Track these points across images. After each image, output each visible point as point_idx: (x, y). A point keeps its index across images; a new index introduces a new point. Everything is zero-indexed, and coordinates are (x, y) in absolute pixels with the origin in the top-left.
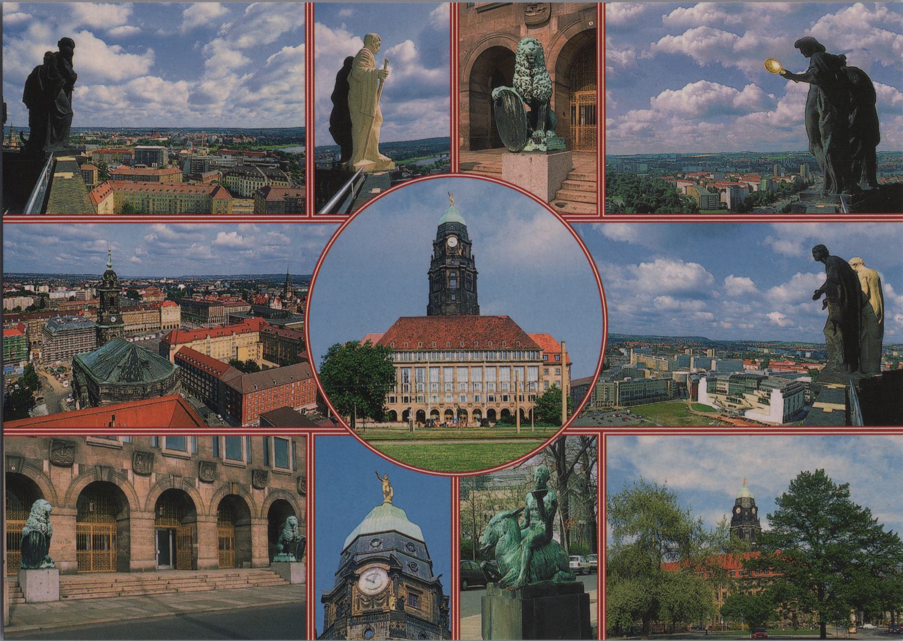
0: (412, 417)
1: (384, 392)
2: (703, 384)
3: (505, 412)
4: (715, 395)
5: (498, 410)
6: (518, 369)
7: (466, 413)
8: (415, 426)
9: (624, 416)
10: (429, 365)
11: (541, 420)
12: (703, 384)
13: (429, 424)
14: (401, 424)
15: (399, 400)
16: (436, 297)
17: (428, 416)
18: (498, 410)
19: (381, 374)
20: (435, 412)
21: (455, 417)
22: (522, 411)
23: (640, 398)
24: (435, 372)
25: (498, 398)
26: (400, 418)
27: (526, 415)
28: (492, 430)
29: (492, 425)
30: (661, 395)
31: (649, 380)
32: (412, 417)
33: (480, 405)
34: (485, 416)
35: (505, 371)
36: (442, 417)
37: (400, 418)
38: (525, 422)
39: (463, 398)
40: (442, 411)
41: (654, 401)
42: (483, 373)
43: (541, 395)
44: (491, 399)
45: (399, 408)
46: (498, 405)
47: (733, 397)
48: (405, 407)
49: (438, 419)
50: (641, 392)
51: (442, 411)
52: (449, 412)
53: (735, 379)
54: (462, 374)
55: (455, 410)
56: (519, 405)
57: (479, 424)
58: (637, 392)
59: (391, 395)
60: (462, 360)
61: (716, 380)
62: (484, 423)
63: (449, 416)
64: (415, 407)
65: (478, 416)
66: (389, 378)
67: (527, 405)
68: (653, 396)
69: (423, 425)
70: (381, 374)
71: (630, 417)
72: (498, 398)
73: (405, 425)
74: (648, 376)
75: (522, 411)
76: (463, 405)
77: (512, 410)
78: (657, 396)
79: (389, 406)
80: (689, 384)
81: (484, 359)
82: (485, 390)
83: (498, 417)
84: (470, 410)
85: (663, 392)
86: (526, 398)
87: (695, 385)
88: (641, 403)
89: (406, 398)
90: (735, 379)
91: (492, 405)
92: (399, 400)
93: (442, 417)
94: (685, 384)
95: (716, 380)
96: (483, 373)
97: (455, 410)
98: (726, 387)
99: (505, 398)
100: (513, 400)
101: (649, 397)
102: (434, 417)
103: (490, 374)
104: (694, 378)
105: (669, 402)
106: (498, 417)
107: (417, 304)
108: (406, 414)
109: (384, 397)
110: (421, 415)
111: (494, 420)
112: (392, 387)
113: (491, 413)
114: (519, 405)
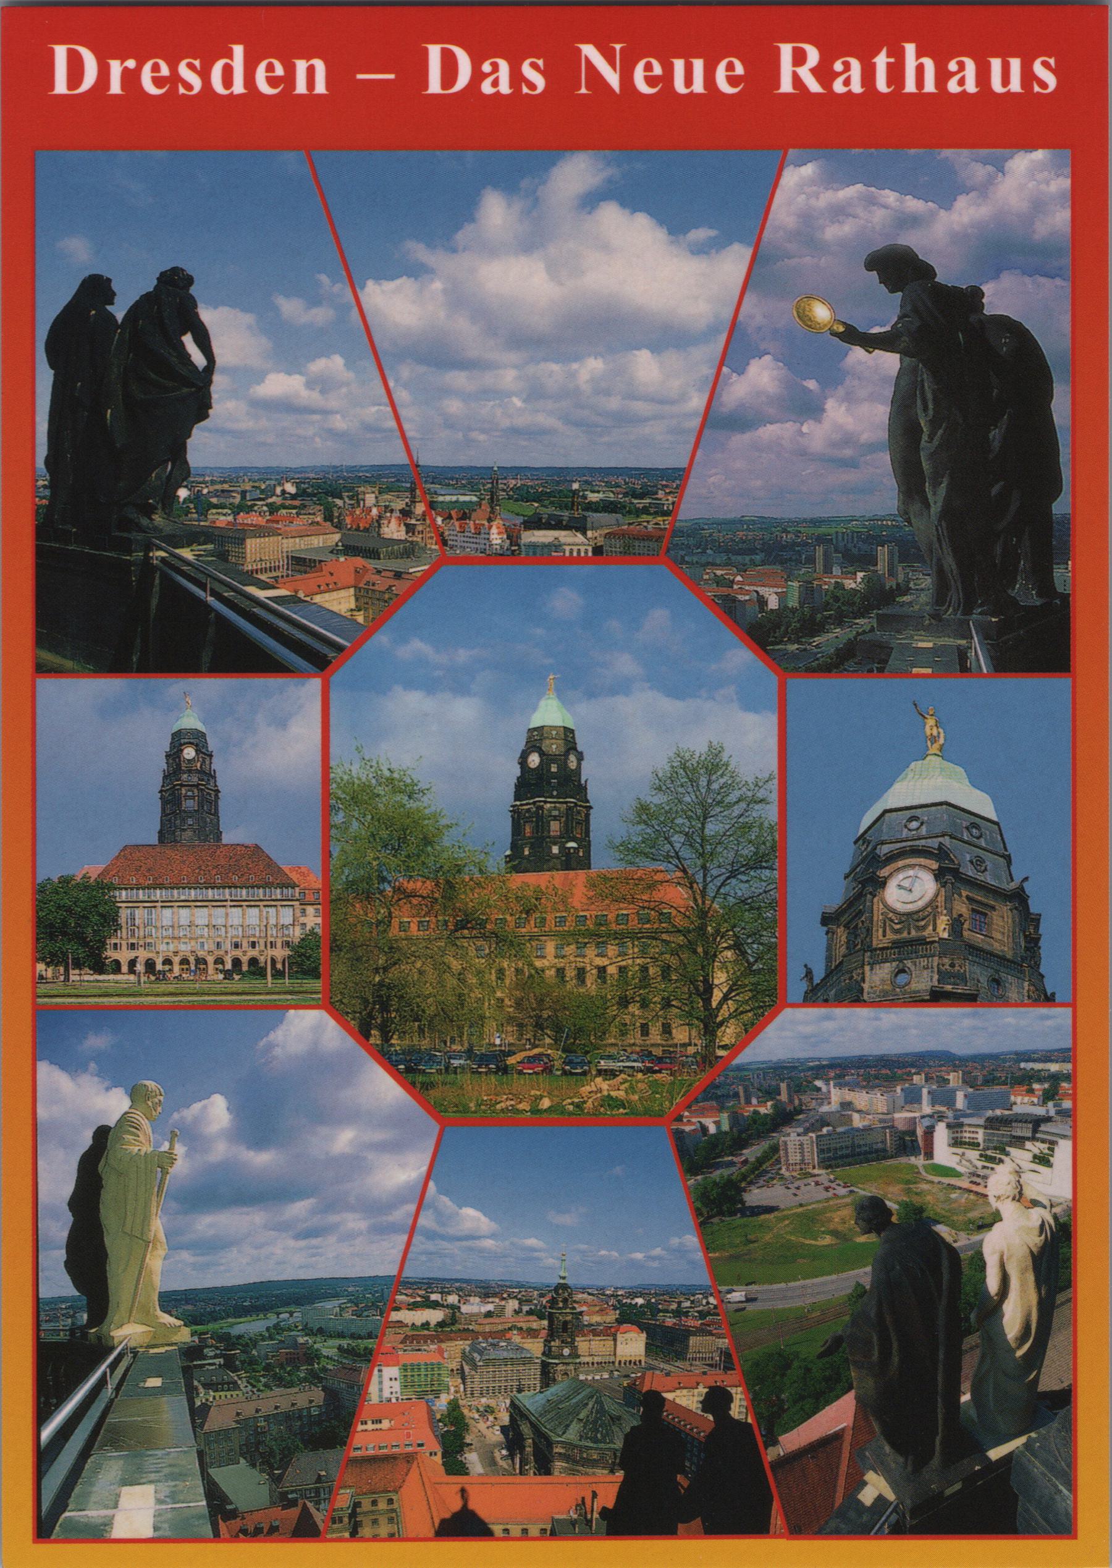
0: (140, 968)
1: (105, 937)
2: (941, 1134)
3: (253, 961)
4: (960, 1151)
5: (245, 960)
6: (270, 909)
7: (205, 963)
8: (143, 979)
9: (827, 1184)
10: (160, 904)
11: (297, 972)
12: (941, 1134)
13: (161, 977)
14: (126, 977)
15: (124, 947)
16: (170, 820)
17: (159, 967)
18: (245, 960)
19: (101, 915)
20: (167, 962)
21: (193, 968)
22: (273, 961)
23: (847, 1156)
24: (167, 913)
25: (245, 944)
26: (125, 969)
27: (279, 966)
28: (237, 983)
29: (237, 977)
30: (877, 1151)
31: (858, 1130)
32: (140, 968)
33: (222, 953)
34: (229, 966)
35: (255, 912)
36: (177, 969)
37: (125, 969)
38: (278, 974)
39: (202, 944)
40: (176, 960)
41: (868, 1161)
42: (227, 914)
43: (297, 941)
44: (236, 946)
45: (124, 956)
46: (245, 952)
47: (989, 1153)
48: (132, 954)
49: (170, 970)
50: (847, 1147)
51: (176, 960)
52: (184, 961)
53: (992, 1123)
54: (202, 916)
55: (192, 959)
56: (270, 952)
57: (221, 976)
58: (842, 1148)
59: (114, 941)
60: (200, 898)
61: (961, 1125)
62: (228, 975)
63: (185, 967)
64: (143, 955)
65: (220, 967)
66: (110, 920)
67: (280, 953)
68: (866, 1153)
69: (153, 978)
70: (101, 915)
71: (833, 1185)
72: (245, 944)
73: (132, 977)
74: (858, 1121)
75: (273, 961)
76: (201, 954)
77: (262, 959)
78: (871, 1153)
79: (111, 954)
80: (920, 1132)
81: (228, 897)
82: (229, 935)
83: (245, 968)
84: (210, 960)
85: (880, 1146)
86: (279, 945)
87: (929, 1132)
88: (850, 1165)
89: (133, 945)
90: (992, 1123)
91: (238, 953)
92: (124, 947)
93: (177, 969)
94: (913, 1133)
95: (961, 1125)
96: (227, 914)
97: (192, 959)
98: (980, 1136)
99: (253, 945)
100: (263, 948)
101: (859, 1154)
102: (167, 967)
103: (235, 915)
104: (927, 1122)
105: (891, 1162)
106: (245, 968)
107: (148, 832)
108: (132, 963)
109: (104, 944)
110: (150, 965)
111: (240, 972)
112: (116, 931)
113: (237, 962)
114: (270, 952)
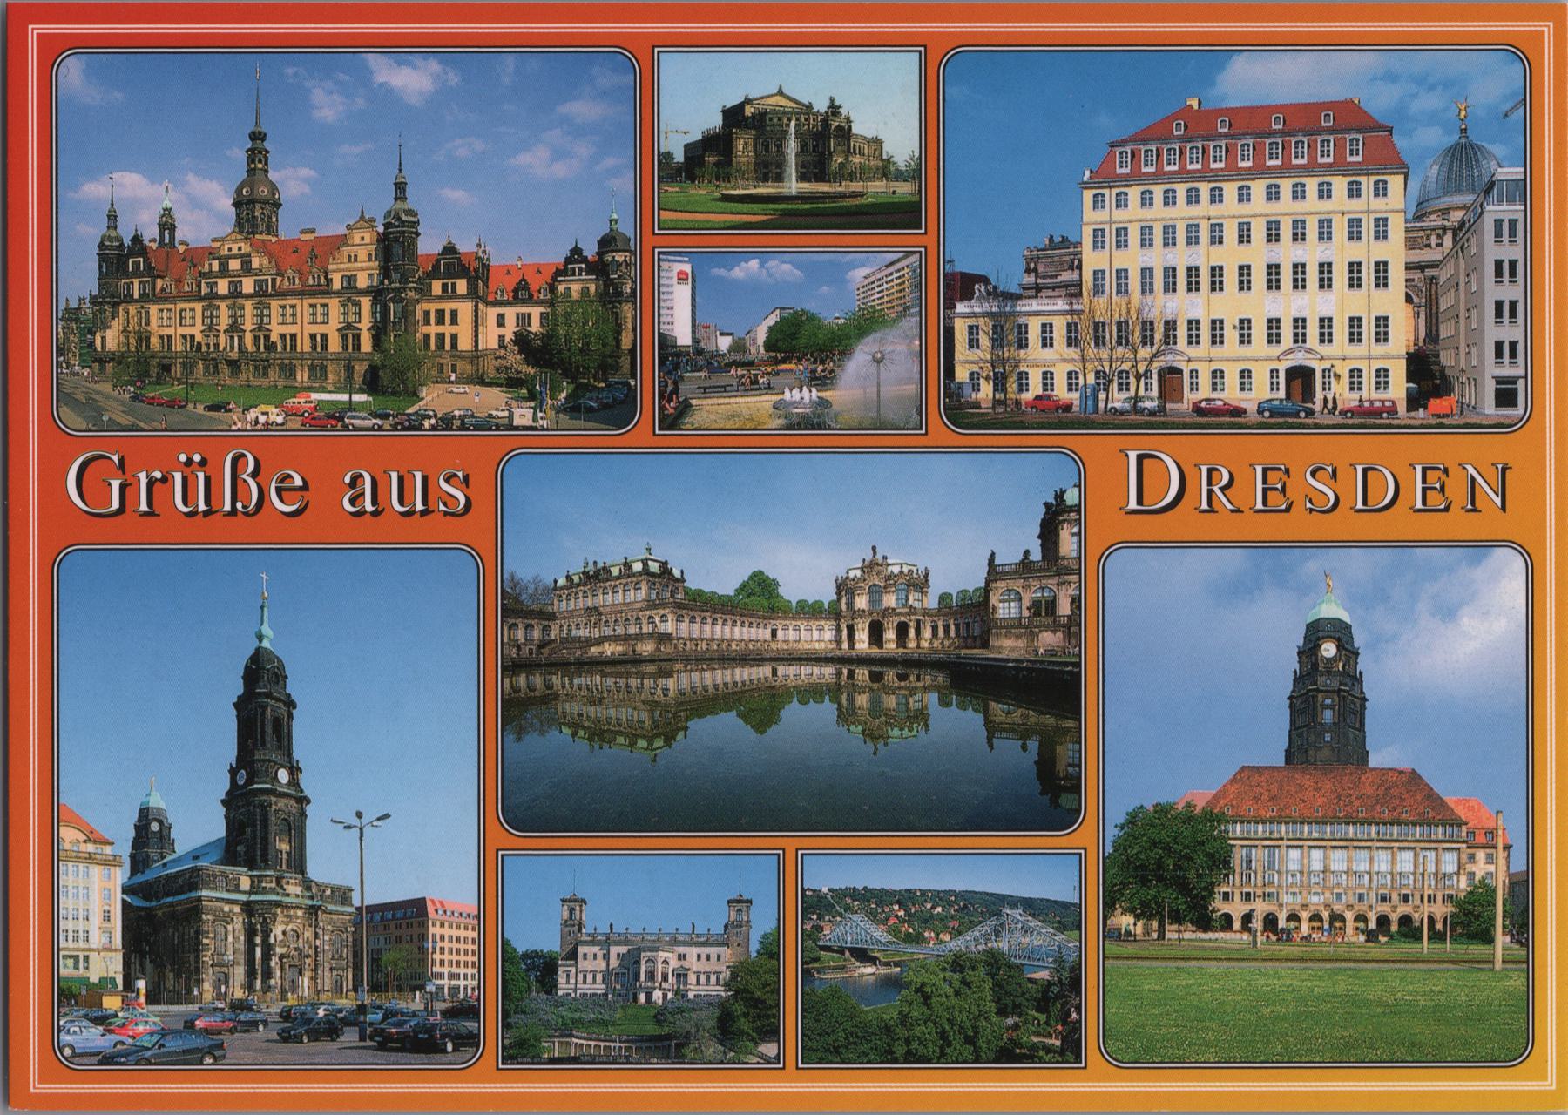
0: (1257, 924)
1: (1212, 884)
3: (1405, 920)
5: (1394, 917)
6: (1428, 853)
7: (1343, 920)
8: (1259, 939)
10: (1285, 843)
11: (1461, 935)
13: (1285, 936)
14: (1238, 936)
15: (1237, 897)
17: (1282, 924)
18: (1394, 917)
19: (1208, 855)
20: (1293, 917)
21: (1326, 926)
22: (1431, 920)
25: (1395, 897)
26: (1237, 925)
27: (1439, 926)
28: (1384, 948)
29: (1383, 939)
32: (1257, 924)
33: (1365, 908)
34: (1372, 925)
35: (1407, 856)
36: (1305, 928)
38: (1437, 937)
39: (1339, 896)
40: (1305, 915)
43: (1462, 895)
44: (1384, 899)
45: (1237, 909)
46: (1395, 907)
48: (1246, 908)
51: (1305, 915)
54: (1338, 860)
55: (1325, 915)
56: (1427, 909)
59: (1224, 889)
62: (1371, 936)
63: (1316, 924)
64: (1261, 908)
65: (1362, 925)
66: (1221, 862)
67: (1441, 910)
69: (1274, 938)
70: (1208, 855)
72: (1395, 897)
73: (1245, 936)
75: (1431, 920)
76: (1337, 908)
77: (1416, 916)
79: (1220, 906)
82: (1374, 885)
83: (1394, 928)
84: (1349, 916)
86: (1439, 898)
89: (1248, 894)
91: (1384, 908)
92: (1237, 897)
93: (1305, 928)
96: (1371, 859)
97: (1325, 915)
99: (1406, 899)
100: (1417, 902)
102: (1292, 925)
106: (1394, 928)
107: (1271, 747)
108: (1247, 918)
109: (1212, 893)
110: (1270, 922)
111: (1388, 933)
112: (1227, 876)
113: (1383, 921)
114: (1427, 909)
